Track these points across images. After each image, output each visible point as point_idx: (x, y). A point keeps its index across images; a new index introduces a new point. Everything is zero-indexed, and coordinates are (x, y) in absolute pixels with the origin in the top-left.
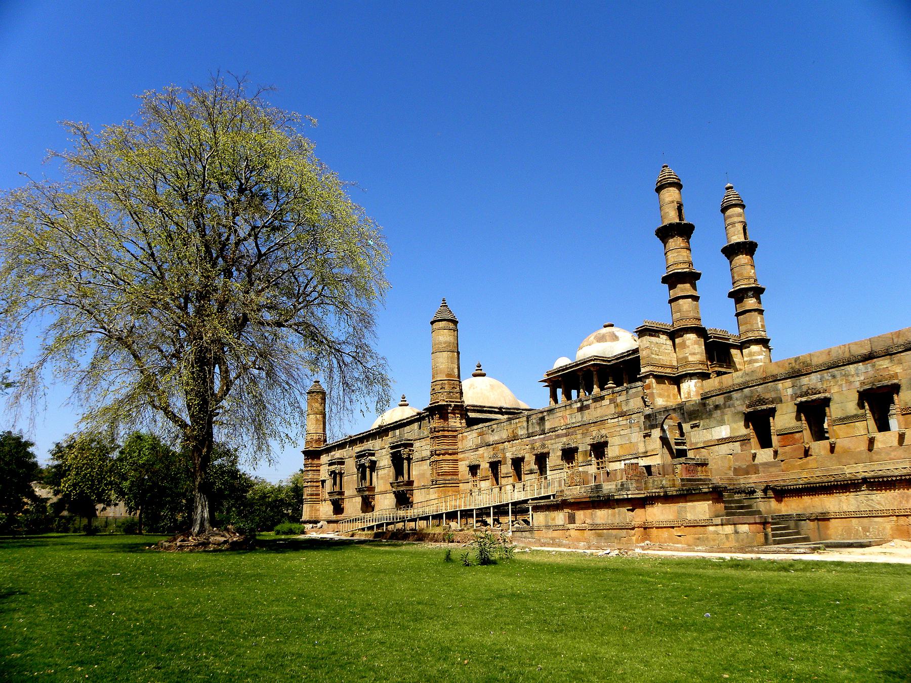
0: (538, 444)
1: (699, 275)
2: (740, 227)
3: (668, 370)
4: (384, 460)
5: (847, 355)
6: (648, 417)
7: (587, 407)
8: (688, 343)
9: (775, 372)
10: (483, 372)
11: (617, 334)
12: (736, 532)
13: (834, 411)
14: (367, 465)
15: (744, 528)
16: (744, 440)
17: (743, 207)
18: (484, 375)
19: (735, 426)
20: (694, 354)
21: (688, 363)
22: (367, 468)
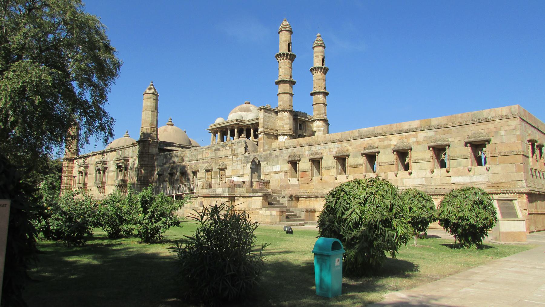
0: (193, 166)
1: (295, 82)
2: (321, 58)
3: (273, 131)
4: (112, 167)
5: (332, 139)
6: (246, 157)
7: (219, 149)
8: (284, 118)
9: (302, 143)
10: (172, 123)
11: (251, 108)
12: (271, 215)
13: (323, 164)
14: (102, 169)
15: (274, 213)
16: (285, 173)
17: (325, 48)
18: (173, 125)
19: (283, 166)
20: (287, 124)
21: (283, 129)
22: (103, 170)
